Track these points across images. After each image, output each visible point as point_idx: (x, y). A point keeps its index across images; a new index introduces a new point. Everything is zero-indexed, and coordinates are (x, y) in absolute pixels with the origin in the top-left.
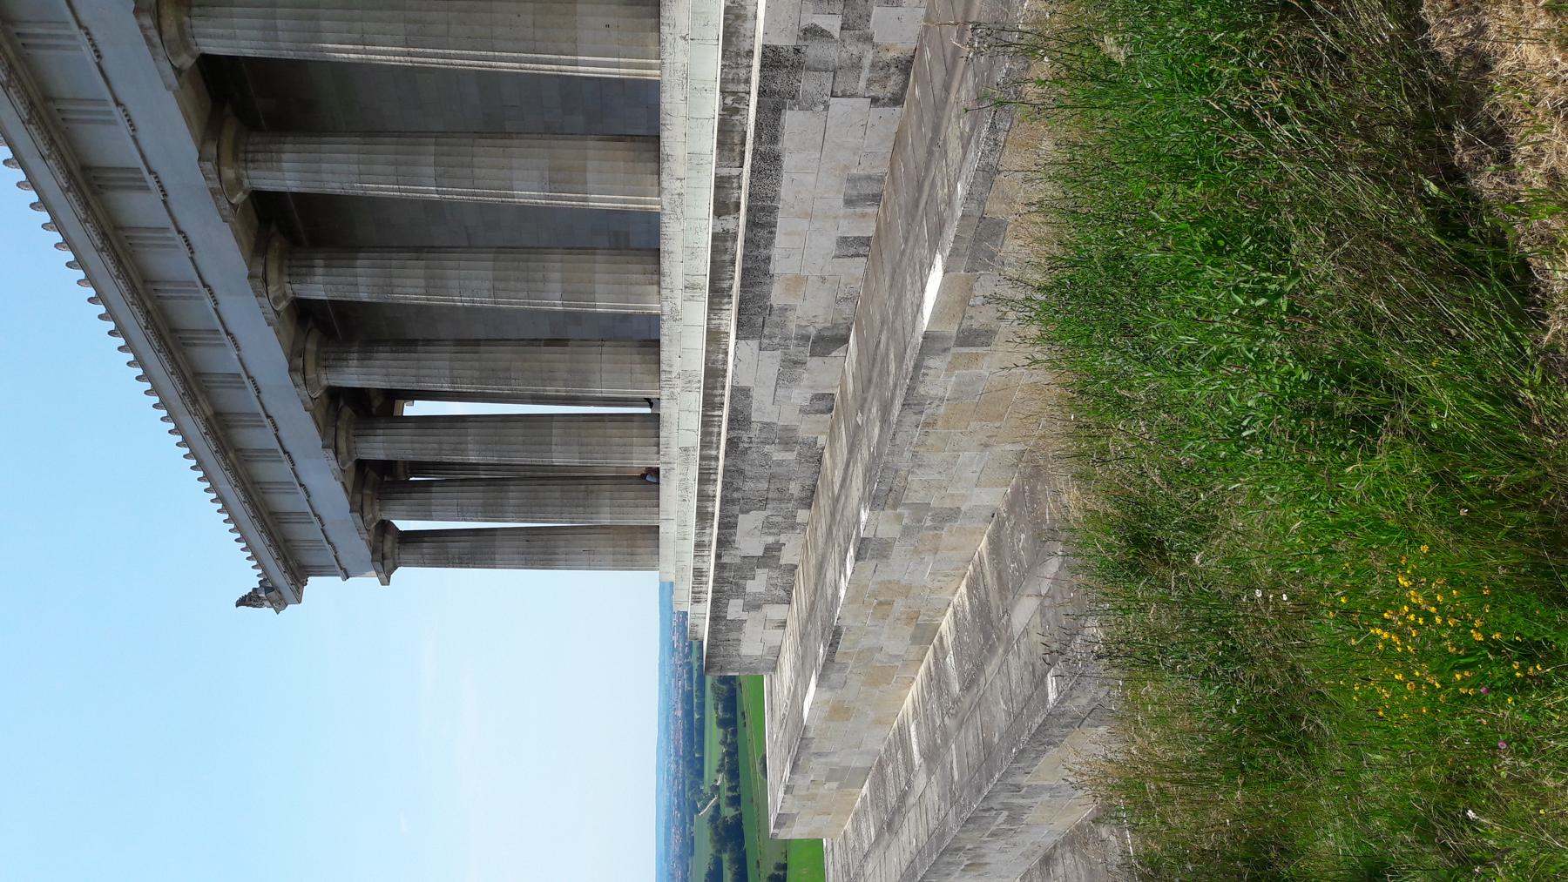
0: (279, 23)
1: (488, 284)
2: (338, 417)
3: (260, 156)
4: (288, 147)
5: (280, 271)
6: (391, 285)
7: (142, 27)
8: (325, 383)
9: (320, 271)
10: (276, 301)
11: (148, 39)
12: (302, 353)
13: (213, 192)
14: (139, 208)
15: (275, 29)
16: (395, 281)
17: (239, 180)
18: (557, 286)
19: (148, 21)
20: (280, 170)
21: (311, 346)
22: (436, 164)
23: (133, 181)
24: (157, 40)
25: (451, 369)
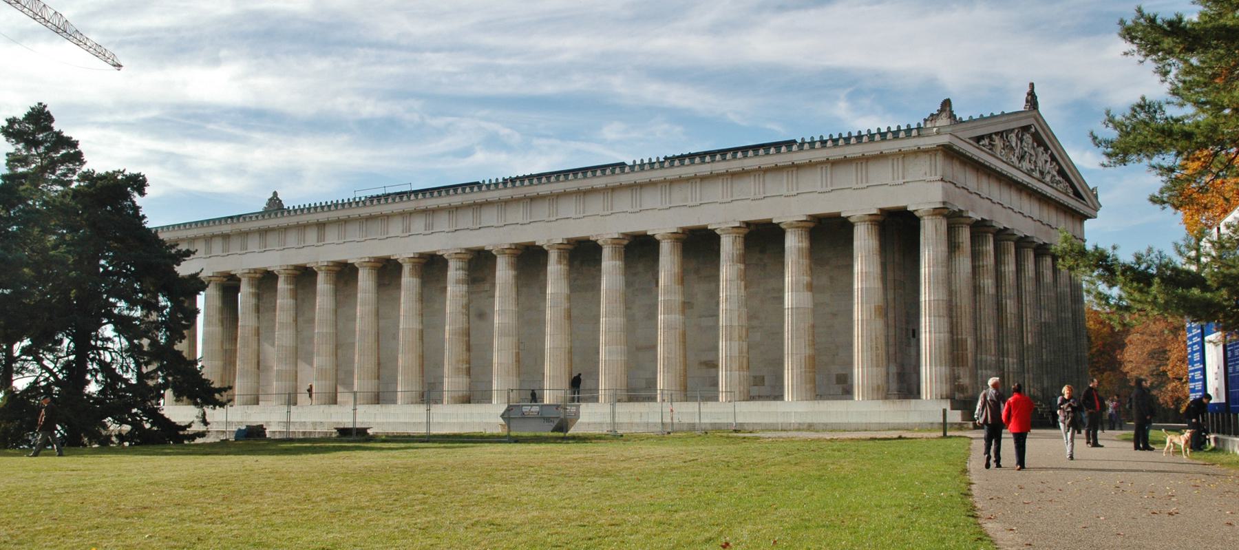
0: (367, 294)
1: (284, 345)
2: (224, 277)
3: (328, 277)
4: (332, 286)
5: (289, 274)
6: (284, 311)
7: (365, 258)
8: (243, 279)
9: (289, 287)
10: (278, 272)
11: (362, 258)
12: (255, 273)
13: (317, 263)
14: (312, 236)
15: (366, 293)
16: (285, 312)
17: (321, 270)
18: (284, 368)
19: (367, 260)
20: (324, 284)
21: (258, 275)
22: (327, 333)
23: (321, 238)
24: (363, 260)
25: (248, 326)
